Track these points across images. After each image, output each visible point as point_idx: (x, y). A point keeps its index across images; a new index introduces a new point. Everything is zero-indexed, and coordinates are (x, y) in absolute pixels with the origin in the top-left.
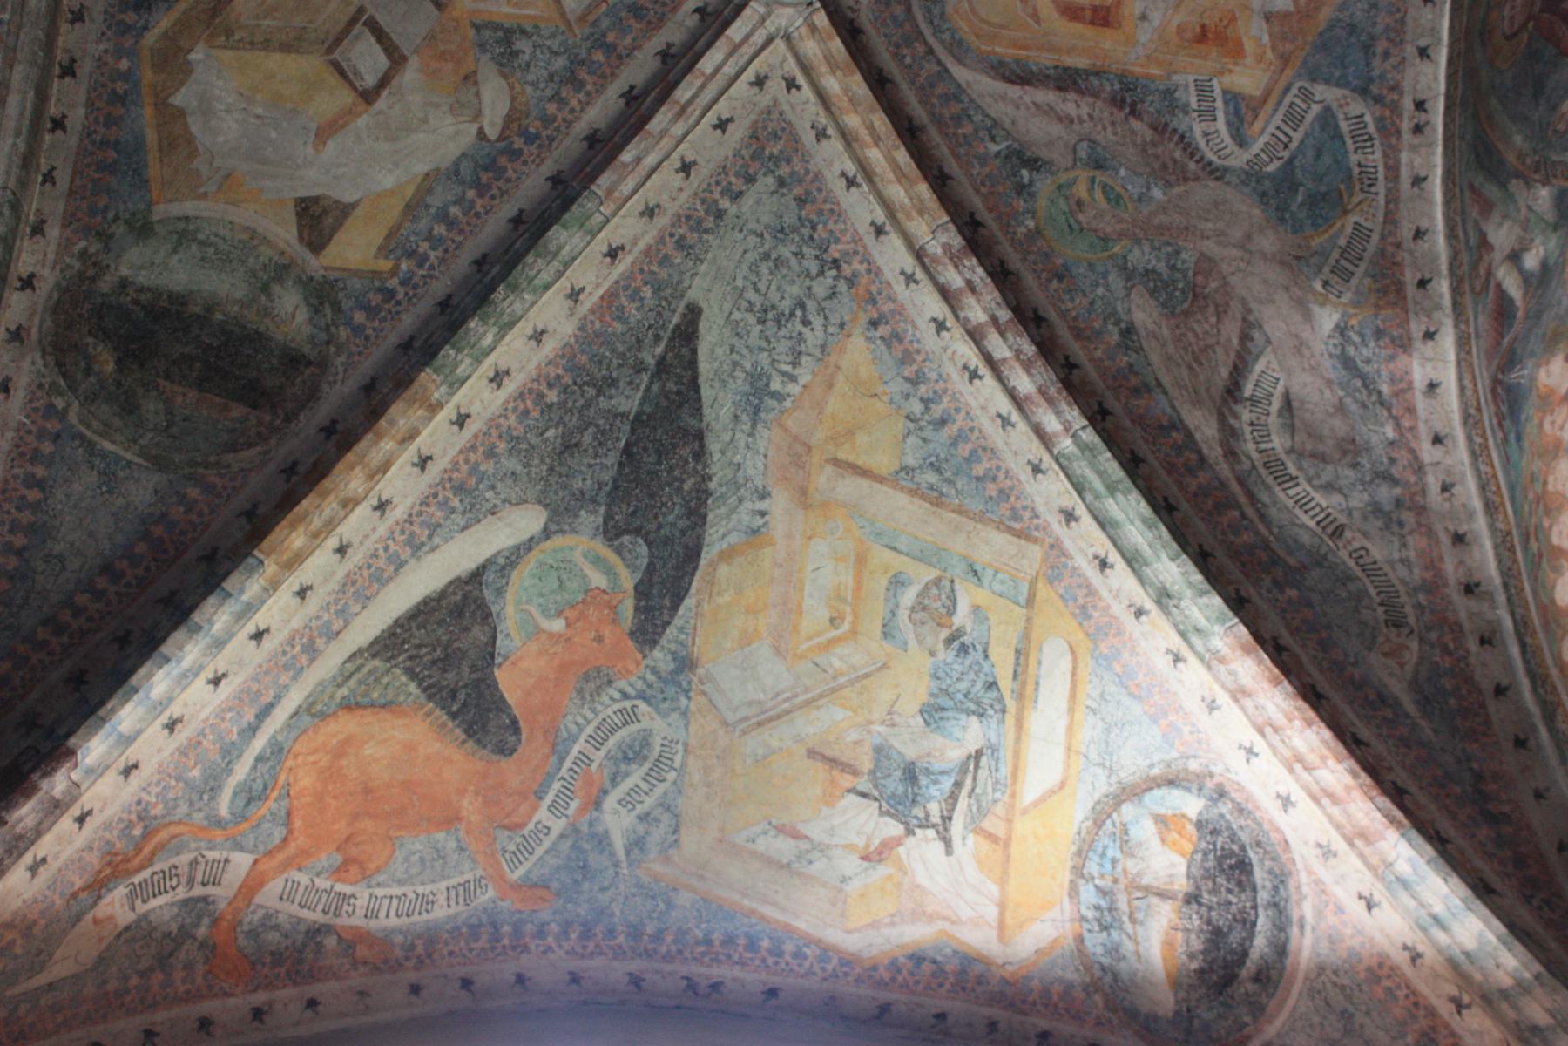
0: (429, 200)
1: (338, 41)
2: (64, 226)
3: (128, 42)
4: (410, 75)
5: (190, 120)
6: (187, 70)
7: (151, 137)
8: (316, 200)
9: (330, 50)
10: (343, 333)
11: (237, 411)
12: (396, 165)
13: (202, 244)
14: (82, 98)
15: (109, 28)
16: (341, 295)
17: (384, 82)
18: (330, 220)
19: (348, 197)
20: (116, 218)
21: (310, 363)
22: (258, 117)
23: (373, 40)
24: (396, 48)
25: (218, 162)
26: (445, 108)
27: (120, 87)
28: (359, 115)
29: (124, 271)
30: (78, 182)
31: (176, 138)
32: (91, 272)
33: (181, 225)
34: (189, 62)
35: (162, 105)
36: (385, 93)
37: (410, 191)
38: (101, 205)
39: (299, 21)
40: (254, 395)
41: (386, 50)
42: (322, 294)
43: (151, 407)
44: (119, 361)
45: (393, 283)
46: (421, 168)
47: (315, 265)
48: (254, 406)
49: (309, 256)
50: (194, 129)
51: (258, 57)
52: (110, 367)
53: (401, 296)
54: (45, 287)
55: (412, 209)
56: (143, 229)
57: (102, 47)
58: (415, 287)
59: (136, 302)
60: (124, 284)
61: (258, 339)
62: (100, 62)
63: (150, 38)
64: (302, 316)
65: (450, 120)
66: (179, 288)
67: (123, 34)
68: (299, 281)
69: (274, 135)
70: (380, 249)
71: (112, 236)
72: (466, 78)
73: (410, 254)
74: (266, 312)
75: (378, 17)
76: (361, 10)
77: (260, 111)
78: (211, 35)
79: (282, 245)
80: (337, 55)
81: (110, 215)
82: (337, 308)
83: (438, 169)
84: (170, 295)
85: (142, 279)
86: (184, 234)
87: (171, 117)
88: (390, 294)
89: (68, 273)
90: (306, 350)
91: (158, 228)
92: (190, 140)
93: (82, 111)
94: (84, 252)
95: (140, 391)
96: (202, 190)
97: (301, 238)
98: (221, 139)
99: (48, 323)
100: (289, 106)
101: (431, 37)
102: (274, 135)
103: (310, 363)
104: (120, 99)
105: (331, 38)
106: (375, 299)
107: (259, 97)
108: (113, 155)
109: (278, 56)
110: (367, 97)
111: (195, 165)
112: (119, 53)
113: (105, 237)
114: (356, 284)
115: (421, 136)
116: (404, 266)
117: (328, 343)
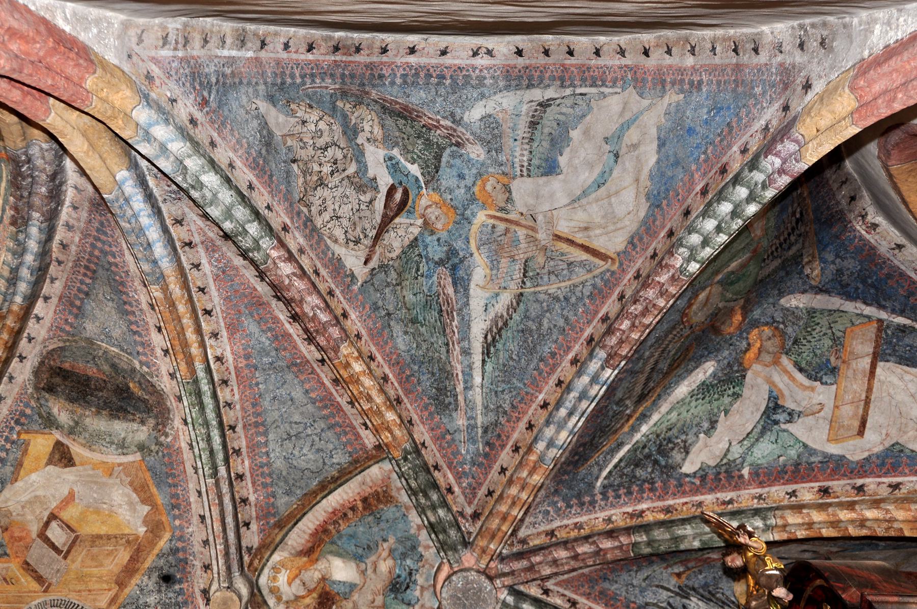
0: (12, 469)
1: (74, 542)
2: (180, 448)
3: (177, 533)
4: (34, 529)
5: (137, 499)
6: (145, 522)
7: (154, 490)
8: (66, 466)
9: (77, 537)
10: (33, 403)
11: (67, 366)
12: (32, 485)
13: (112, 443)
14: (193, 506)
15: (189, 539)
16: (40, 421)
17: (47, 524)
18: (57, 456)
19: (51, 468)
20: (157, 453)
21: (43, 389)
22: (105, 503)
23: (56, 544)
24: (44, 541)
25: (118, 481)
26: (14, 514)
27: (176, 512)
28: (57, 507)
29: (144, 428)
30: (182, 468)
31: (141, 489)
32: (160, 427)
33: (125, 451)
34: (147, 526)
35: (154, 505)
36: (45, 519)
37: (22, 472)
38: (166, 458)
39: (95, 550)
40: (64, 374)
41: (49, 540)
42: (49, 422)
43: (106, 368)
44: (129, 388)
45: (18, 428)
46: (19, 484)
47: (57, 435)
48: (60, 368)
49: (61, 439)
50: (135, 495)
51: (112, 532)
52: (131, 385)
53: (12, 422)
54: (177, 423)
55: (19, 465)
56: (141, 447)
57: (190, 530)
58: (7, 426)
59: (134, 415)
60: (143, 422)
61: (72, 400)
62: (189, 522)
63: (167, 536)
64: (55, 411)
65: (11, 508)
66: (117, 421)
67: (181, 537)
68: (62, 427)
69: (95, 495)
70: (29, 444)
71: (156, 444)
72: (7, 529)
73: (13, 442)
74: (72, 412)
75: (56, 555)
76: (65, 558)
77: (105, 506)
78: (137, 540)
79: (76, 444)
80: (73, 535)
81: (160, 454)
82: (41, 416)
83: (12, 484)
84: (119, 418)
85: (135, 426)
86: (122, 447)
87: (147, 499)
88: (17, 422)
89: (169, 426)
90: (47, 396)
91: (136, 449)
92: (135, 490)
93: (192, 500)
94: (167, 435)
95: (113, 374)
96: (121, 468)
97: (68, 448)
98: (121, 492)
99: (169, 404)
100: (91, 509)
101: (28, 548)
102: (95, 495)
103: (43, 389)
104: (174, 507)
105: (77, 543)
106: (23, 420)
107: (107, 512)
108: (170, 481)
109: (102, 533)
110: (53, 517)
111: (129, 479)
112: (181, 528)
113: (159, 443)
114: (35, 427)
115: (23, 500)
116: (15, 436)
117: (38, 399)
